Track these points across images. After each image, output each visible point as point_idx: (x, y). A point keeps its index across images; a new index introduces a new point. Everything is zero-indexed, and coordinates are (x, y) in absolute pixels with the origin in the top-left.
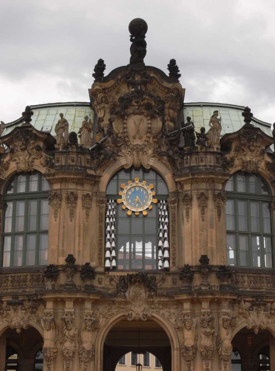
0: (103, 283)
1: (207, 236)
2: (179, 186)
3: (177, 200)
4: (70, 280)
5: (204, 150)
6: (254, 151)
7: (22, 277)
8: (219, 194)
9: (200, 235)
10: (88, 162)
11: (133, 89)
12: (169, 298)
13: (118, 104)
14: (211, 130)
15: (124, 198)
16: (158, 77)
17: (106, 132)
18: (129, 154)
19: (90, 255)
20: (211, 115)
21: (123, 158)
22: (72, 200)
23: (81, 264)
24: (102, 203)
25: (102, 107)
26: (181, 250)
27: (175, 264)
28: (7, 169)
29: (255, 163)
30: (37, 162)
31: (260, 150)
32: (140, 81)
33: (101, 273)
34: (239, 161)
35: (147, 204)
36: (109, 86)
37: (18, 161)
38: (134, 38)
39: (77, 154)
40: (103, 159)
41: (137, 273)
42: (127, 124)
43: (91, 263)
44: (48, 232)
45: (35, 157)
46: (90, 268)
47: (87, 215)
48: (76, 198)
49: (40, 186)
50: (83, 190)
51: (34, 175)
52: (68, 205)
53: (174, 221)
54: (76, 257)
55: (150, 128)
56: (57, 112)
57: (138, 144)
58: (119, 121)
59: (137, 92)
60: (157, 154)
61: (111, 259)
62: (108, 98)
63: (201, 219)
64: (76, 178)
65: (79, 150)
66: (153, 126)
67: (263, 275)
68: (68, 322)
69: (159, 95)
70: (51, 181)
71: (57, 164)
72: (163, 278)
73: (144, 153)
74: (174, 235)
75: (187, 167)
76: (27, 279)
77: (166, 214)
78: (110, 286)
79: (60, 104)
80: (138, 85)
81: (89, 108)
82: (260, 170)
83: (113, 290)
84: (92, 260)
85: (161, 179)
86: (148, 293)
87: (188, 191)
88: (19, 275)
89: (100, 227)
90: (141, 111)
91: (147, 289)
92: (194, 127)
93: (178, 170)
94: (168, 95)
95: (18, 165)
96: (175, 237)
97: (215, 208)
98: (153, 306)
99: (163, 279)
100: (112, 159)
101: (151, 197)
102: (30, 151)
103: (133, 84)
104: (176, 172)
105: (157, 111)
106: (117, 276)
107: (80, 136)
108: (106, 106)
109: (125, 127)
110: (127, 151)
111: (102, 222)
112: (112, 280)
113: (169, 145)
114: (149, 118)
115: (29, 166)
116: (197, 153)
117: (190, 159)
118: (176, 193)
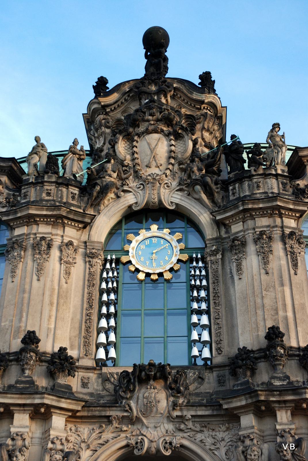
0: (89, 385)
2: (223, 230)
4: (26, 375)
5: (261, 172)
8: (292, 234)
9: (263, 297)
10: (73, 198)
11: (147, 101)
12: (213, 410)
13: (125, 122)
19: (70, 339)
22: (43, 249)
26: (232, 327)
33: (87, 369)
36: (112, 102)
39: (57, 186)
40: (99, 193)
48: (49, 246)
53: (216, 281)
57: (155, 173)
58: (126, 145)
68: (14, 450)
70: (12, 224)
71: (23, 201)
72: (201, 376)
75: (236, 199)
77: (203, 273)
78: (104, 392)
83: (108, 398)
86: (172, 399)
89: (90, 293)
91: (170, 392)
96: (220, 307)
98: (182, 426)
99: (200, 377)
106: (117, 374)
108: (108, 131)
111: (93, 286)
113: (204, 171)
116: (250, 177)
117: (239, 188)
118: (218, 240)
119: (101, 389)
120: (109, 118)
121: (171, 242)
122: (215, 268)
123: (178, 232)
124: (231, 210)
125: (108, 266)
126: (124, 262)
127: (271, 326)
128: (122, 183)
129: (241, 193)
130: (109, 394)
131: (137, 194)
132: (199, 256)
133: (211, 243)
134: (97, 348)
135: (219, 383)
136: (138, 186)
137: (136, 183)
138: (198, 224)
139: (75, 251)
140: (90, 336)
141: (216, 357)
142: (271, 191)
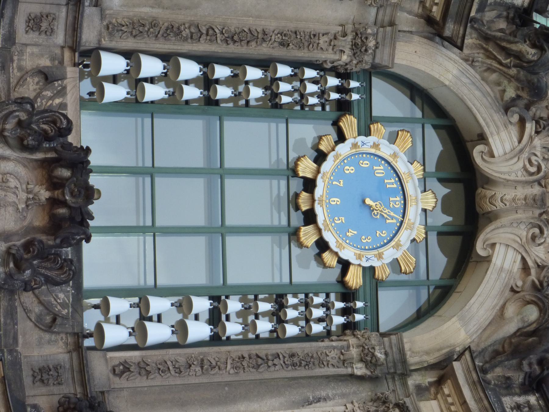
3: (378, 372)
15: (363, 144)
21: (515, 140)
24: (354, 46)
27: (120, 375)
40: (518, 56)
60: (541, 283)
72: (59, 321)
73: (534, 226)
77: (317, 328)
78: (16, 71)
89: (264, 33)
91: (18, 243)
96: (232, 371)
99: (54, 320)
106: (63, 106)
110: (536, 155)
111: (283, 44)
119: (23, 63)
121: (393, 243)
122: (328, 358)
123: (417, 263)
125: (333, 81)
126: (341, 124)
128: (541, 118)
130: (12, 85)
131: (515, 156)
132: (359, 317)
133: (391, 347)
134: (127, 54)
135: (40, 370)
136: (533, 158)
137: (542, 153)
138: (437, 314)
140: (157, 36)
141: (106, 360)
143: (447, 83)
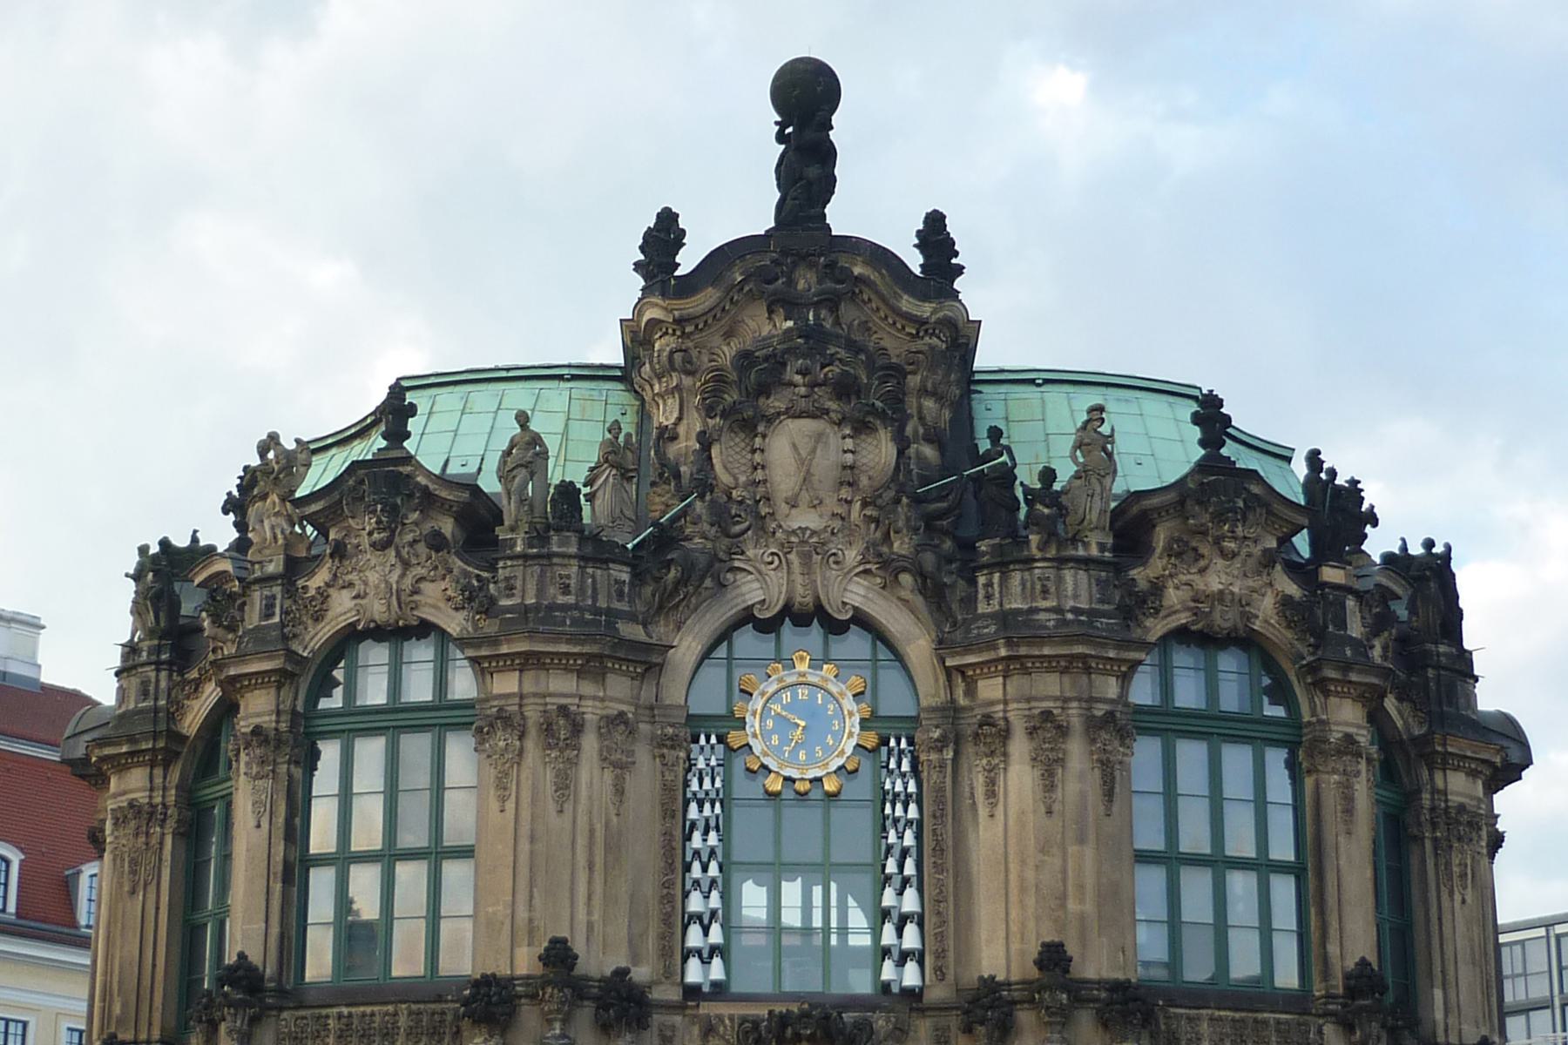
1: (1064, 871)
3: (951, 736)
5: (1052, 553)
6: (1234, 555)
7: (377, 1019)
10: (620, 595)
11: (790, 324)
13: (733, 376)
14: (1077, 476)
15: (753, 726)
16: (880, 274)
17: (685, 480)
18: (772, 563)
19: (630, 941)
20: (1075, 425)
21: (750, 577)
22: (562, 737)
23: (594, 972)
24: (673, 747)
25: (671, 386)
26: (965, 922)
27: (943, 974)
28: (318, 618)
29: (1240, 601)
30: (432, 591)
31: (1257, 550)
32: (814, 295)
34: (1180, 593)
35: (839, 749)
37: (359, 587)
38: (789, 130)
39: (582, 564)
40: (678, 583)
41: (806, 1006)
42: (766, 454)
43: (633, 969)
44: (473, 851)
45: (423, 572)
46: (632, 986)
47: (619, 791)
48: (577, 728)
49: (441, 683)
50: (602, 700)
51: (418, 639)
52: (549, 752)
54: (579, 947)
55: (852, 468)
56: (500, 404)
57: (807, 528)
58: (737, 440)
59: (806, 332)
61: (705, 955)
62: (694, 353)
63: (1043, 809)
64: (580, 655)
65: (589, 550)
66: (865, 460)
67: (1266, 1015)
69: (883, 343)
71: (504, 602)
73: (828, 561)
74: (939, 868)
75: (992, 616)
76: (399, 1028)
77: (912, 788)
79: (511, 374)
80: (808, 306)
81: (620, 386)
82: (1255, 628)
84: (636, 958)
85: (893, 657)
87: (992, 703)
88: (368, 1009)
90: (816, 405)
92: (1015, 465)
93: (954, 624)
94: (919, 345)
95: (363, 602)
97: (1093, 769)
99: (900, 1030)
100: (708, 582)
101: (853, 726)
102: (404, 553)
103: (786, 303)
104: (949, 632)
105: (878, 404)
106: (731, 1018)
107: (590, 498)
108: (687, 381)
109: (758, 464)
111: (673, 817)
112: (710, 1030)
113: (922, 530)
114: (847, 431)
115: (403, 605)
116: (1029, 562)
117: (1001, 585)
118: (950, 711)
120: (690, 344)
124: (981, 651)
127: (1048, 939)
129: (1005, 599)
131: (764, 579)
133: (931, 719)
134: (685, 959)
139: (630, 733)
142: (1071, 603)
143: (700, 647)
